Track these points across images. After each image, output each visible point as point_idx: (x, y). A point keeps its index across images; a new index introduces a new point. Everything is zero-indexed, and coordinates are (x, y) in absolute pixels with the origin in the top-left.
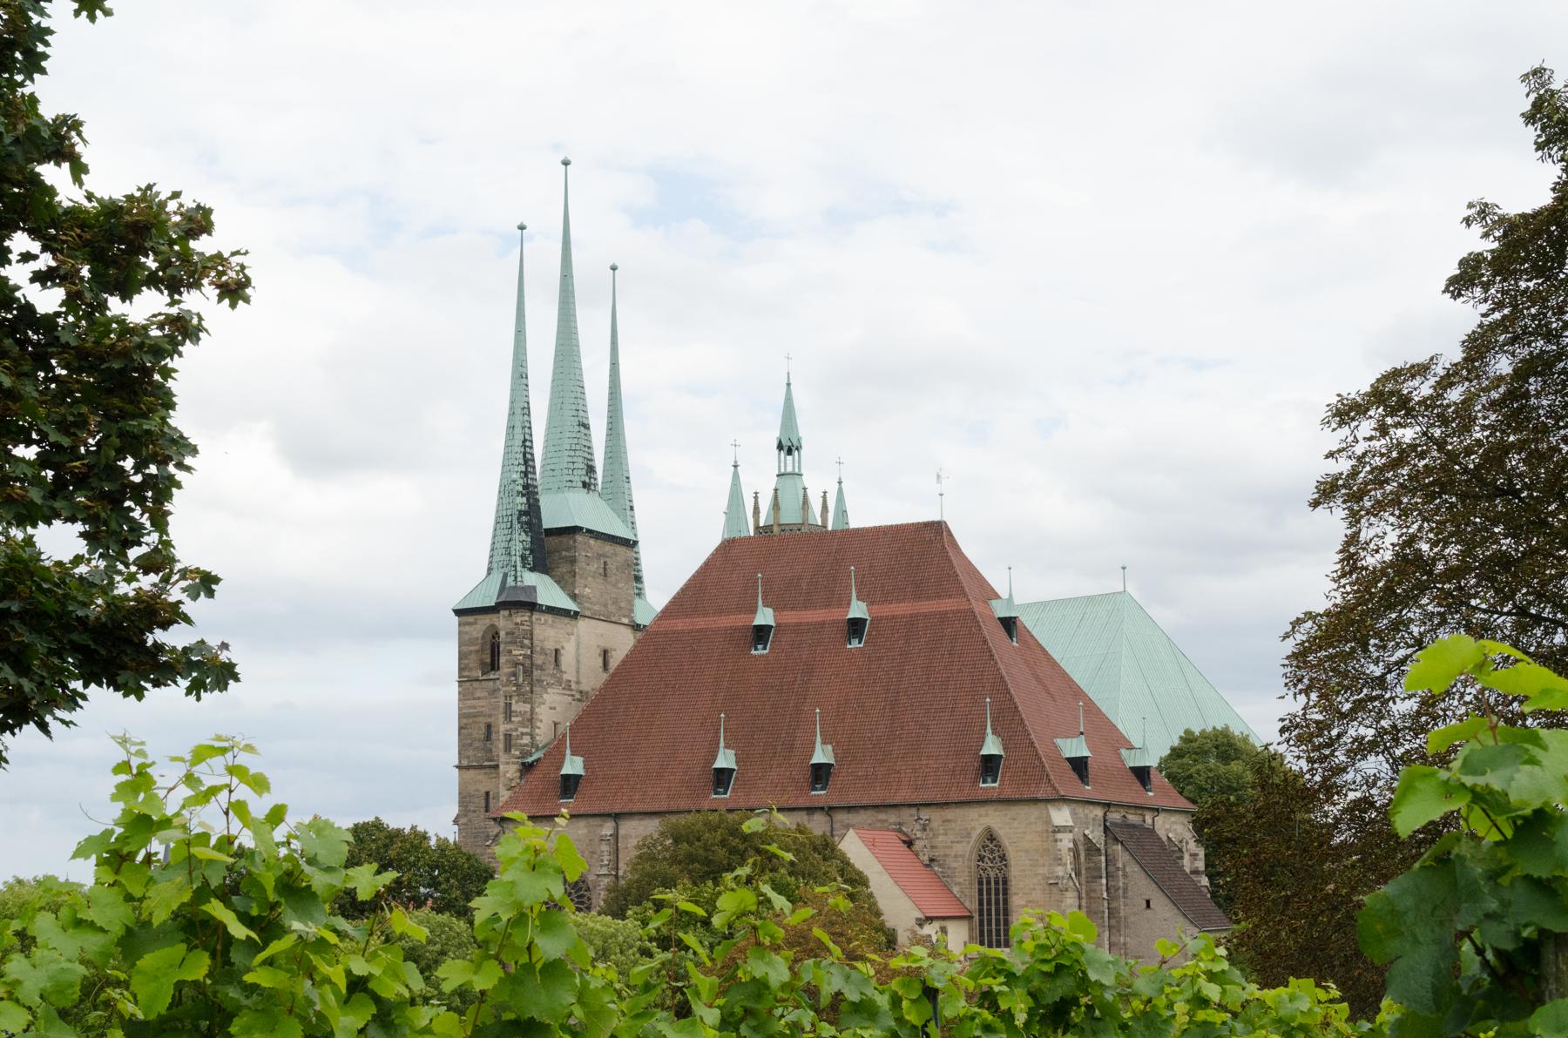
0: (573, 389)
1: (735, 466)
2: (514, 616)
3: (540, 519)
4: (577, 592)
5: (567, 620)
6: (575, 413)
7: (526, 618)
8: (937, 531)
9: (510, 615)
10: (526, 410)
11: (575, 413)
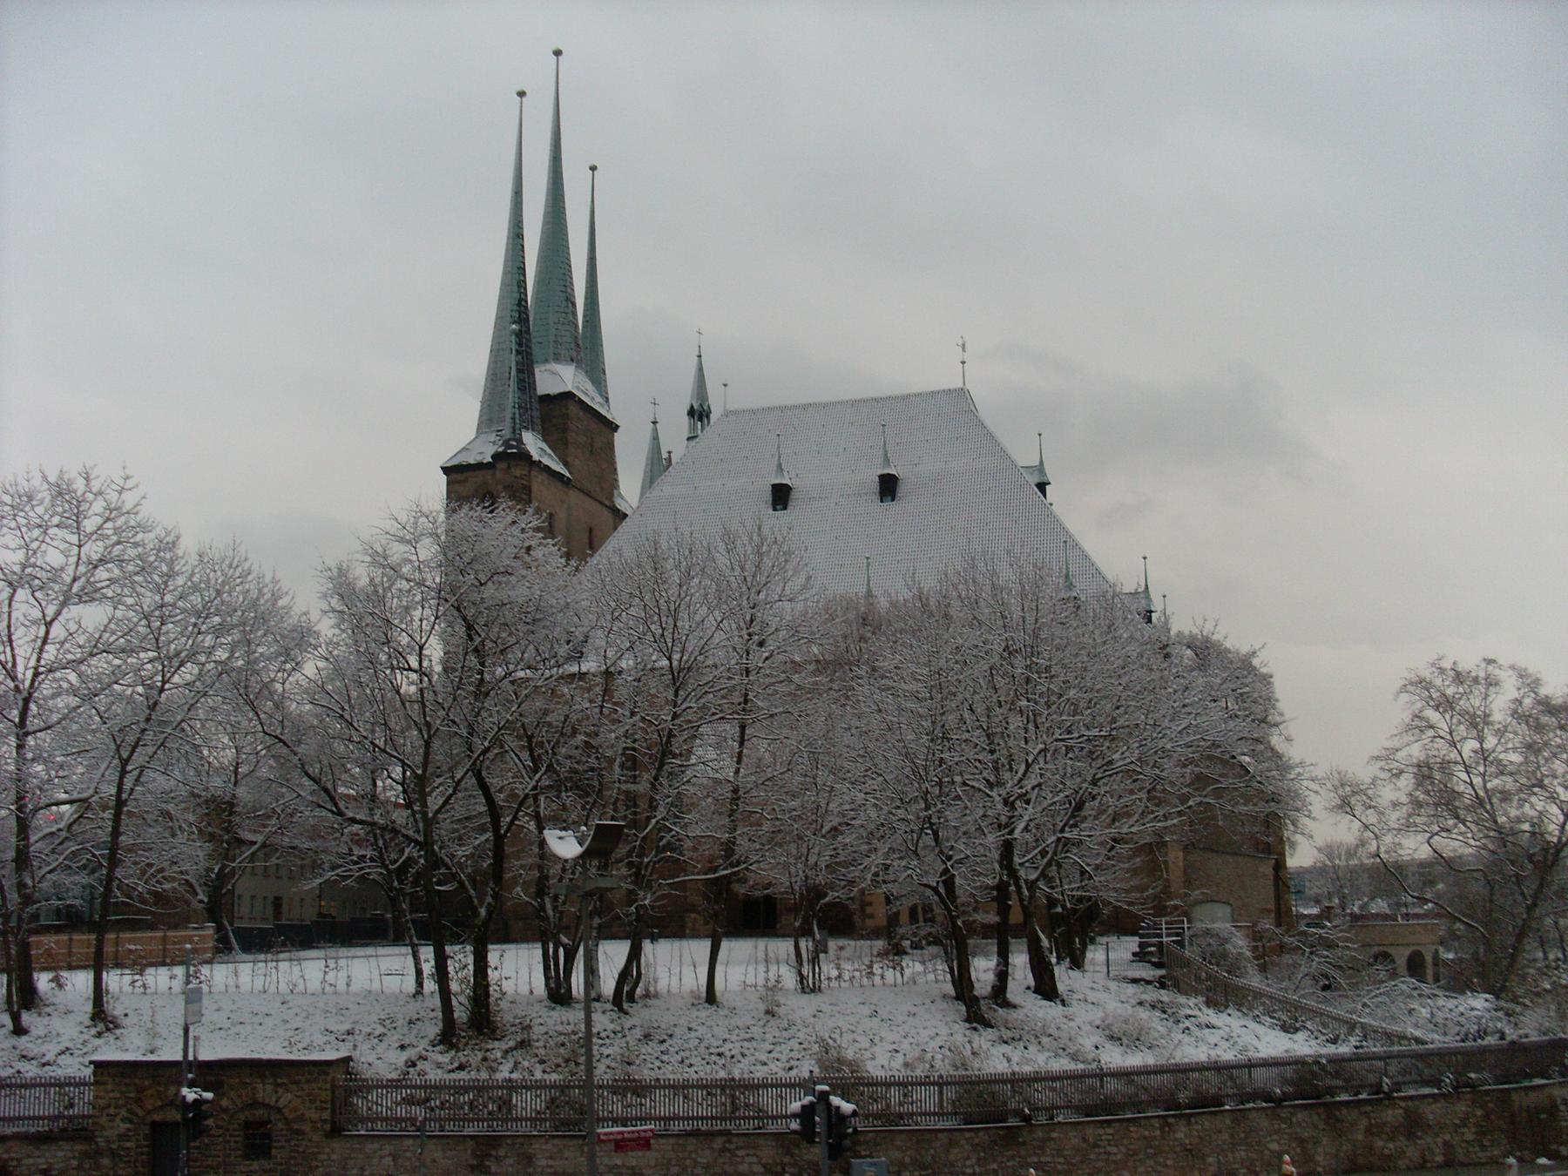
0: (561, 265)
1: (655, 423)
2: (513, 470)
3: (535, 389)
4: (568, 459)
5: (559, 485)
6: (563, 289)
7: (524, 472)
8: (961, 394)
9: (509, 467)
10: (522, 270)
11: (563, 289)
